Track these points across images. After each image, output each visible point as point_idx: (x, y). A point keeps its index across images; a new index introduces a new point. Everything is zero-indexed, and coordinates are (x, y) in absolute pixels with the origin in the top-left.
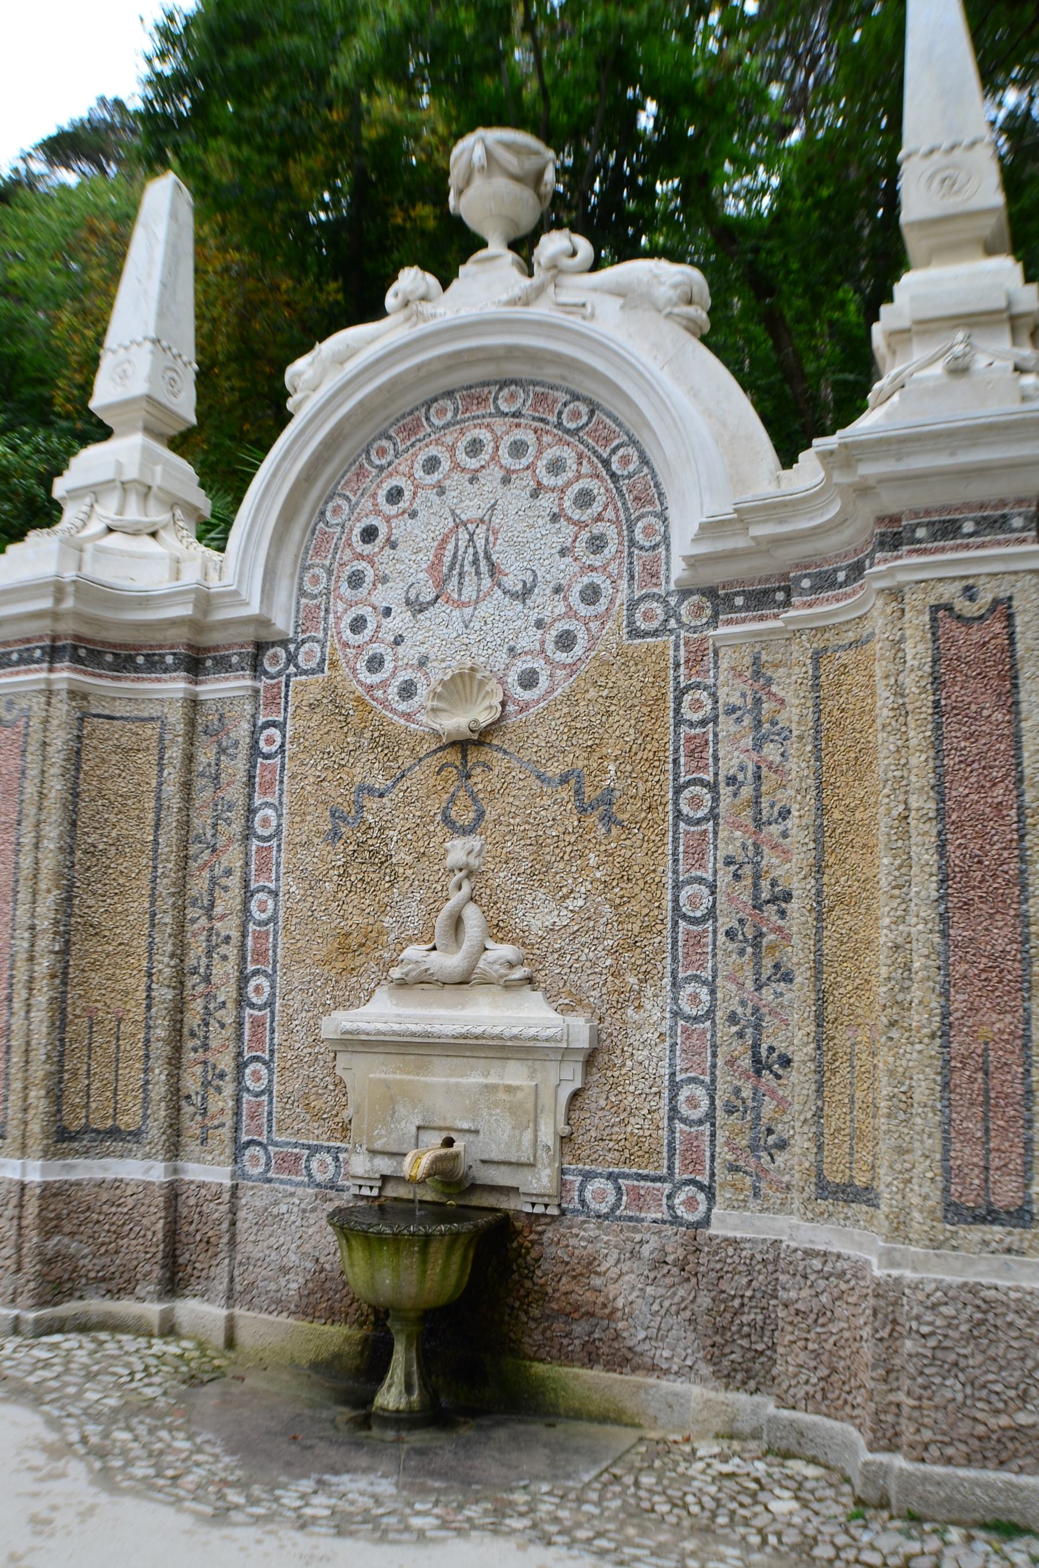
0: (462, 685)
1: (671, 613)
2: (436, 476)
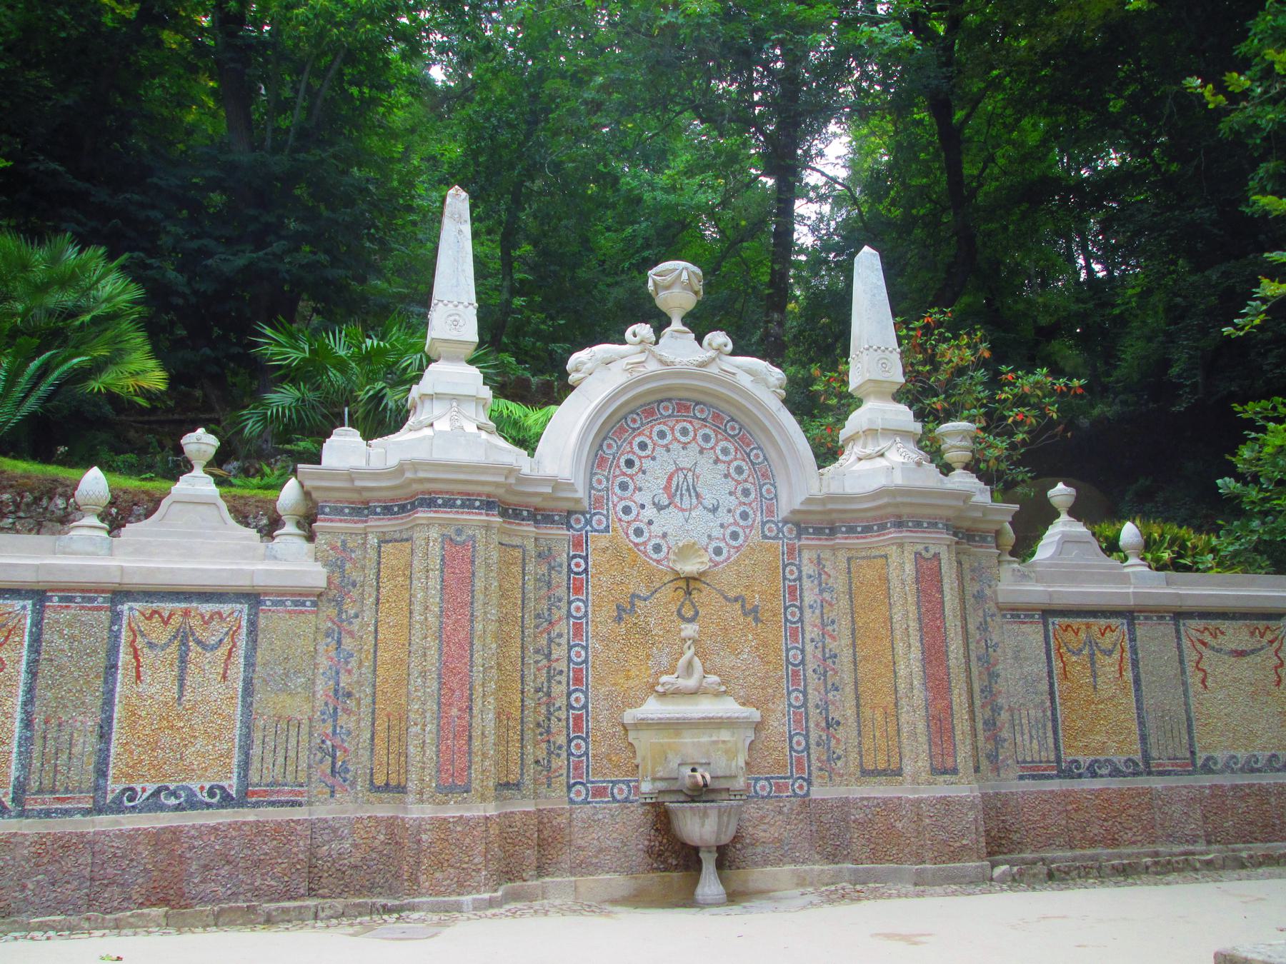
0: (686, 551)
1: (780, 530)
2: (665, 442)
